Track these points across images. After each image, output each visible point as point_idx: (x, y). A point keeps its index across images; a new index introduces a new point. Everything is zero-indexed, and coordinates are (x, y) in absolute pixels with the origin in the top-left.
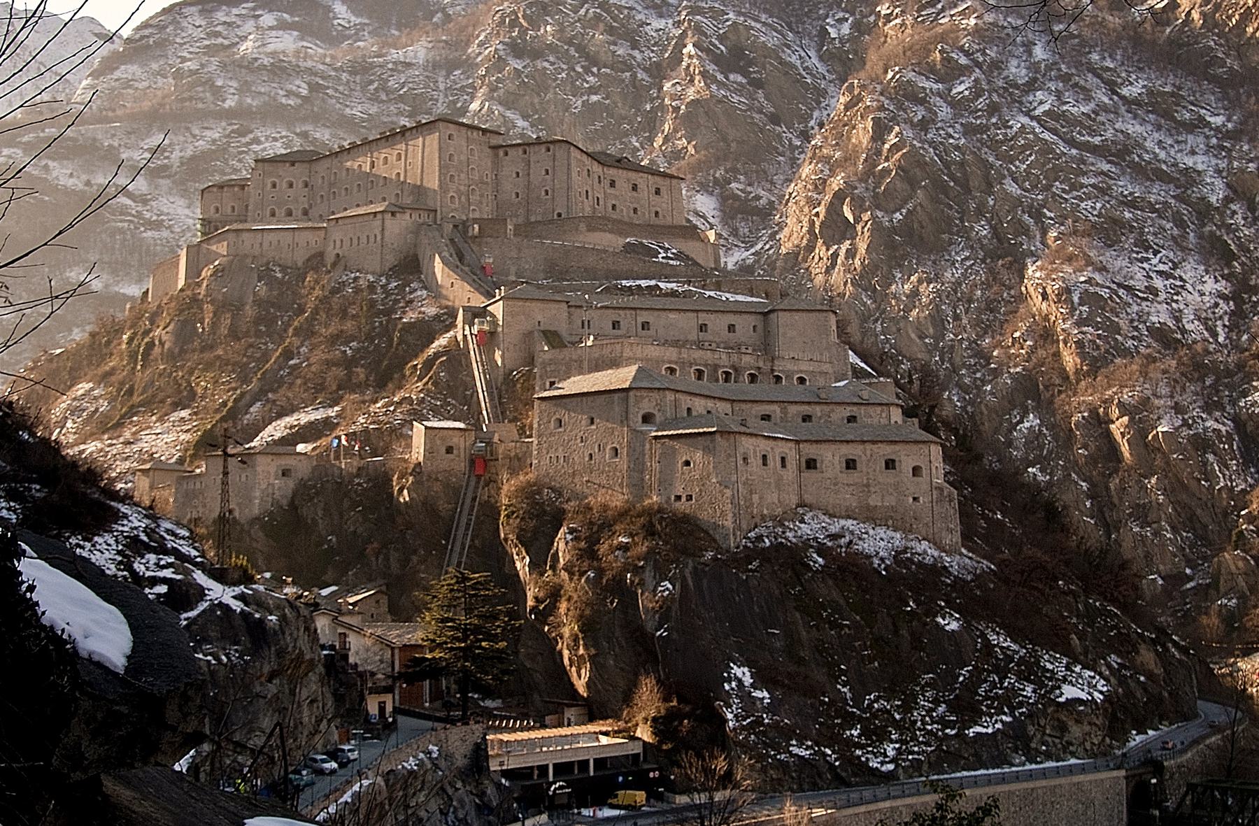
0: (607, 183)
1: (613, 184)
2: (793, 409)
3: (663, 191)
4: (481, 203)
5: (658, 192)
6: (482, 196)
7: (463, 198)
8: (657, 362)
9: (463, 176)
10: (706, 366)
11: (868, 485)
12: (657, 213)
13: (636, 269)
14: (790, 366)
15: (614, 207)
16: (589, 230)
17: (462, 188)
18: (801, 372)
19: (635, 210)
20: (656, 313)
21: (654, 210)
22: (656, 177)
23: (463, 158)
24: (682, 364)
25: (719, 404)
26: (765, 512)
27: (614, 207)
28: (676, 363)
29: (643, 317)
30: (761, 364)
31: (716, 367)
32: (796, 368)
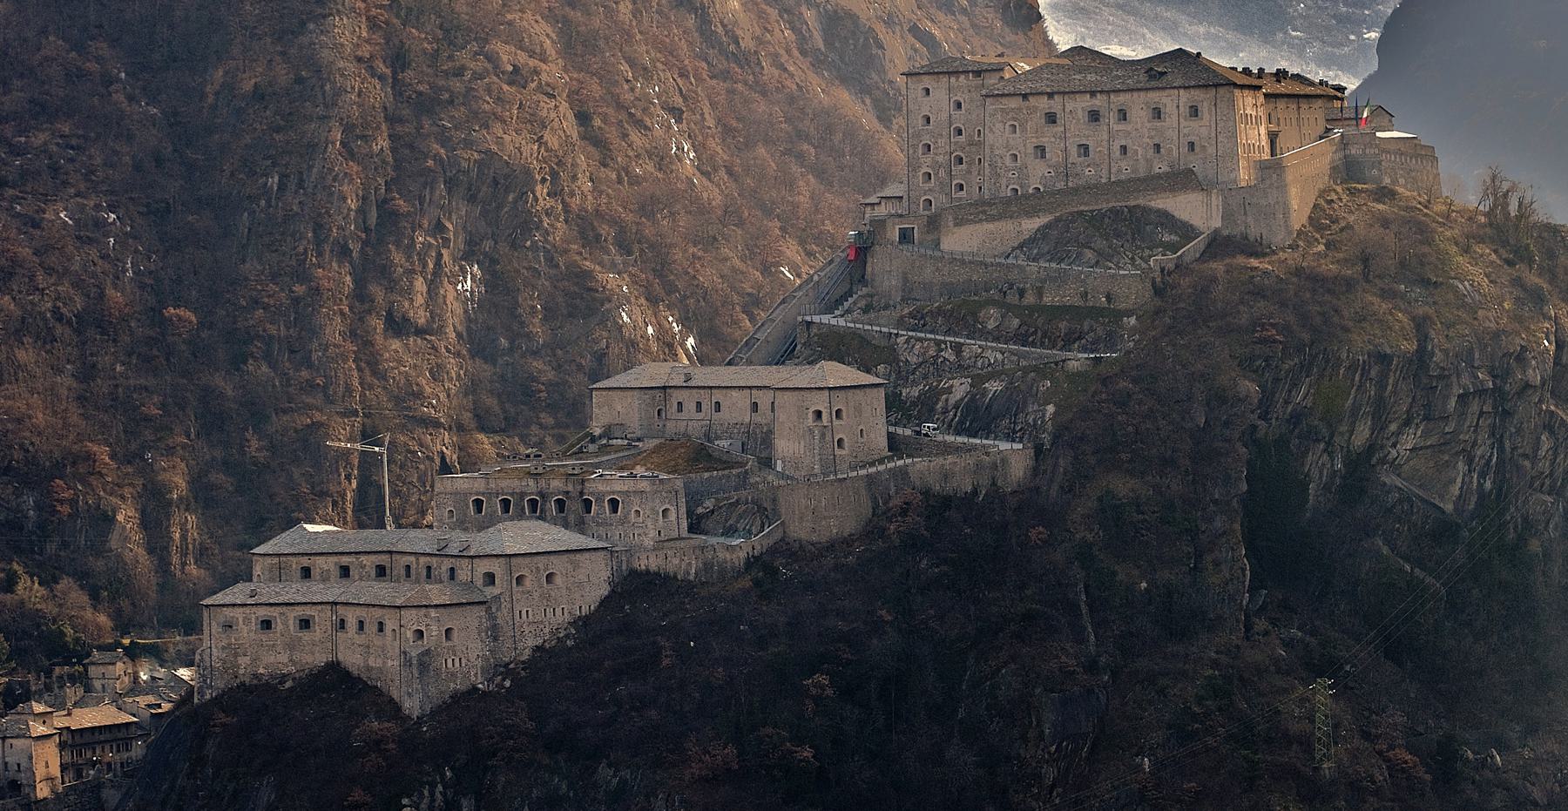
0: (1113, 117)
1: (1123, 115)
2: (422, 560)
3: (1205, 109)
4: (969, 172)
5: (1194, 112)
6: (970, 164)
7: (942, 173)
8: (465, 494)
9: (941, 142)
10: (512, 494)
11: (368, 647)
12: (1192, 145)
13: (975, 278)
14: (601, 487)
15: (1124, 149)
16: (956, 225)
17: (940, 159)
18: (613, 493)
19: (1157, 147)
20: (724, 391)
21: (1184, 141)
22: (1192, 91)
23: (945, 116)
24: (489, 495)
25: (363, 558)
26: (261, 671)
27: (1124, 149)
28: (483, 494)
29: (718, 396)
30: (570, 488)
31: (522, 495)
32: (608, 488)
